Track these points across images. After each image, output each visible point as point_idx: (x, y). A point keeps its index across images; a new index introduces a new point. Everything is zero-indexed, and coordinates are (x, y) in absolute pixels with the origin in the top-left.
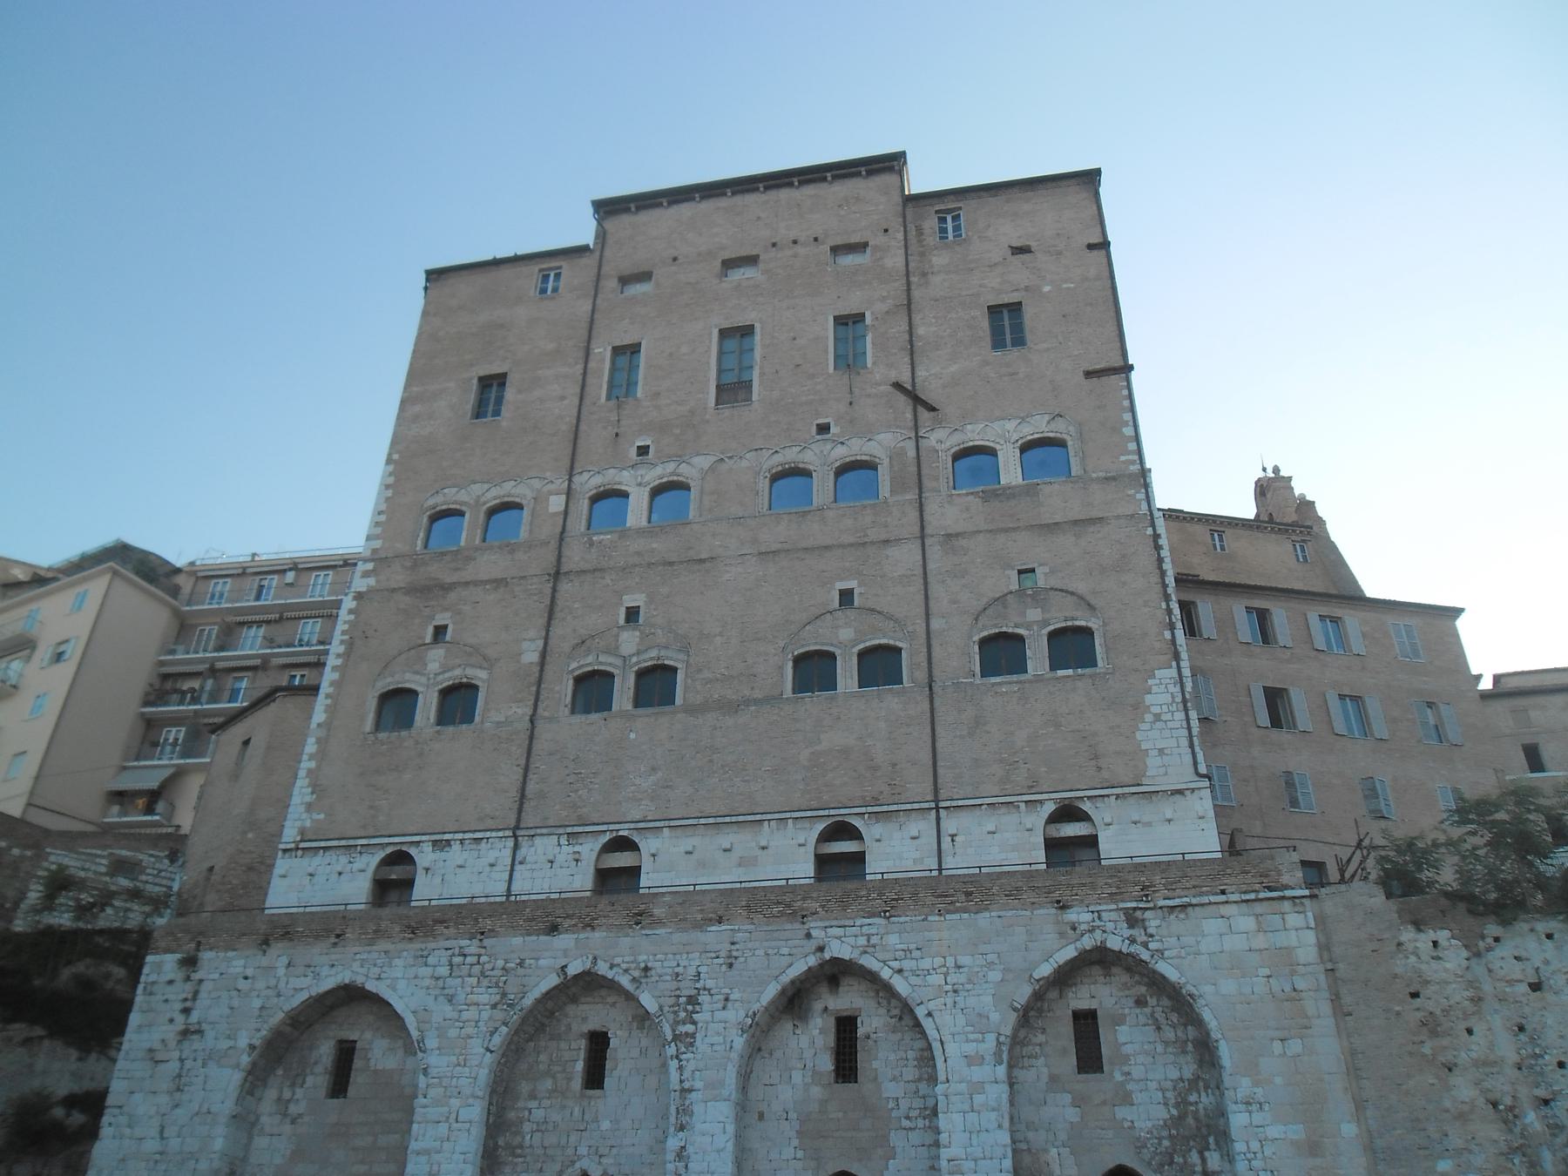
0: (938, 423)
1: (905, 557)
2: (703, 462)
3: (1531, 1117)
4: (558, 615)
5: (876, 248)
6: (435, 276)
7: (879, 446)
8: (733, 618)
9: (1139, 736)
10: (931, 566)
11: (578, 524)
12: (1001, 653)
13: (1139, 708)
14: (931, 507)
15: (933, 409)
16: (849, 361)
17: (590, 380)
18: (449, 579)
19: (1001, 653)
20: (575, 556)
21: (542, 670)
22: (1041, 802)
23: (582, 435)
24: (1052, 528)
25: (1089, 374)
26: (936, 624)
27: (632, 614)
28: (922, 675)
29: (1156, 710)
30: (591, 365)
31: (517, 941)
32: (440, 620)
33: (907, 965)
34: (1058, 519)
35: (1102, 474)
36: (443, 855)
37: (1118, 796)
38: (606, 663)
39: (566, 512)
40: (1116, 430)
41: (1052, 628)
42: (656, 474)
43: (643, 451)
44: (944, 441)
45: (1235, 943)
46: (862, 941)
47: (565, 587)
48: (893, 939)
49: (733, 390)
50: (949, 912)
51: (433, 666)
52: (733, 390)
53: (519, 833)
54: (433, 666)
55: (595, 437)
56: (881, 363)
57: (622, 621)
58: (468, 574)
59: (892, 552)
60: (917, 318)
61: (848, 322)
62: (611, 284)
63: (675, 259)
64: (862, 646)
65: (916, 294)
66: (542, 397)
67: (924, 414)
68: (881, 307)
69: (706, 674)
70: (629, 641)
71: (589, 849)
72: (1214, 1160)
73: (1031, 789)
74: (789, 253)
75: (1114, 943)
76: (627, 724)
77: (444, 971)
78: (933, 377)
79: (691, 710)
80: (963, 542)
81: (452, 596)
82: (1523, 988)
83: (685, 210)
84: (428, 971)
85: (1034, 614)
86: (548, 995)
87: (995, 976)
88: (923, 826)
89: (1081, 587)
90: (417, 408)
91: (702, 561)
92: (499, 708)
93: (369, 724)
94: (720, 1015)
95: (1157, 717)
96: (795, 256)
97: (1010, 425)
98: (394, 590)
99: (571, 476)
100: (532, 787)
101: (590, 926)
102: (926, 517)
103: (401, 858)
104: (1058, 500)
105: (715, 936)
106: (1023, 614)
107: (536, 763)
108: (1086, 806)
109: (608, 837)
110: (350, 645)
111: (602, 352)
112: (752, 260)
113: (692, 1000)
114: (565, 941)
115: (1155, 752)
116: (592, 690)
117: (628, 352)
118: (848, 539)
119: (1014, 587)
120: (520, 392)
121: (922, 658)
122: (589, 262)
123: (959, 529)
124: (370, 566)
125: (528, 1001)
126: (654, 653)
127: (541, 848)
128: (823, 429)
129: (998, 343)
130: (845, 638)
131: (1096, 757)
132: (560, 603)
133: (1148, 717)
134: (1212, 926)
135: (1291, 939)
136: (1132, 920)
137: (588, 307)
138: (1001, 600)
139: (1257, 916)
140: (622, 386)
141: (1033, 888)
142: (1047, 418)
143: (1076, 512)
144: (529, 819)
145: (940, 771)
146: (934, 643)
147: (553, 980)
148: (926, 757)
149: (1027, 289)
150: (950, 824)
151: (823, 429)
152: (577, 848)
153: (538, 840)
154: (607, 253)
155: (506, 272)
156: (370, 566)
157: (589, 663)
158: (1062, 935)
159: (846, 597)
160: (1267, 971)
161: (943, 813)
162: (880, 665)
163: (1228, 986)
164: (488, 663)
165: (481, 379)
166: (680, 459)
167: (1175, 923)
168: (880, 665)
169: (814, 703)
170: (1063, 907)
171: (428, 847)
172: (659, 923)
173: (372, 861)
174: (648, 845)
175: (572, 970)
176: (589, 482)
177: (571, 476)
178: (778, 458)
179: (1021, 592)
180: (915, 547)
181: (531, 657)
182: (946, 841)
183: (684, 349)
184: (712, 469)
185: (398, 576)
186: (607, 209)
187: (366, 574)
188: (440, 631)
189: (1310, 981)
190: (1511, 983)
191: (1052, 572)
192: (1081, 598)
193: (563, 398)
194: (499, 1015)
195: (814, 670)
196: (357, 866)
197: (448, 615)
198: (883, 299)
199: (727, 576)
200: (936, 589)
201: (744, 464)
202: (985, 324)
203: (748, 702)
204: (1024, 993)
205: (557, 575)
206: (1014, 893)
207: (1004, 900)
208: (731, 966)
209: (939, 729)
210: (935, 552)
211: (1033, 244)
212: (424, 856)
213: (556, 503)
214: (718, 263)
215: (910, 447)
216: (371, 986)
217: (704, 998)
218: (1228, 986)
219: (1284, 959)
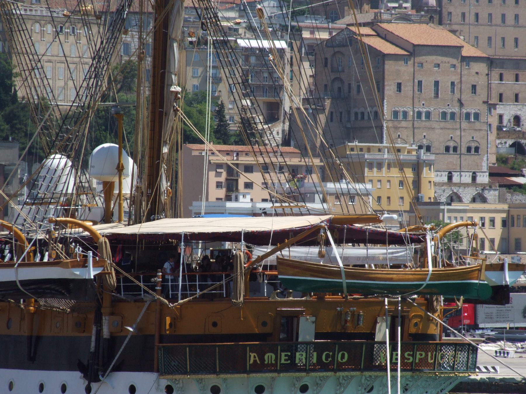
1: (458, 132)
7: (456, 110)
16: (453, 91)
18: (399, 126)
19: (469, 149)
24: (476, 130)
27: (425, 136)
32: (399, 133)
43: (423, 104)
44: (464, 111)
47: (415, 130)
55: (416, 100)
59: (457, 131)
61: (453, 84)
70: (425, 140)
81: (400, 129)
85: (473, 144)
88: (459, 173)
89: (479, 141)
104: (478, 125)
111: (416, 81)
117: (420, 83)
118: (451, 127)
123: (465, 128)
130: (452, 144)
136: (483, 190)
137: (413, 70)
140: (420, 90)
143: (479, 128)
150: (462, 173)
151: (448, 105)
189: (497, 198)
203: (440, 154)
206: (472, 185)
213: (411, 113)
219: (495, 196)
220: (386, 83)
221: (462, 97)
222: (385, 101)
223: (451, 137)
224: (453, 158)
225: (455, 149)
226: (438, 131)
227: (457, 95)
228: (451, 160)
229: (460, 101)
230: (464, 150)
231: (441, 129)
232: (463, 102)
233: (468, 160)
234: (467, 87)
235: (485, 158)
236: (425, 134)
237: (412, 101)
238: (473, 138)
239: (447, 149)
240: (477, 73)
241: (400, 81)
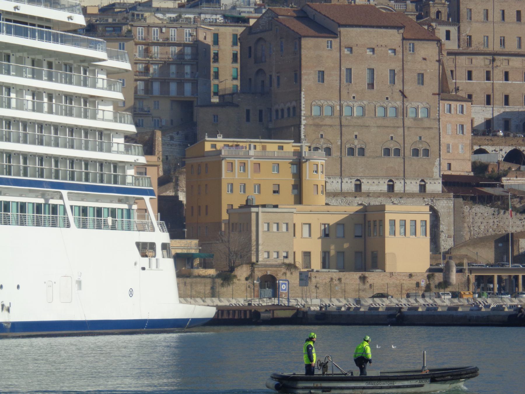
0: (407, 101)
1: (401, 131)
3: (472, 228)
4: (343, 135)
8: (374, 139)
10: (405, 134)
12: (416, 152)
13: (434, 164)
14: (406, 120)
16: (393, 82)
17: (342, 77)
18: (321, 123)
19: (416, 152)
24: (424, 128)
25: (433, 94)
26: (406, 145)
27: (356, 136)
30: (342, 72)
32: (322, 133)
34: (425, 126)
38: (352, 146)
43: (354, 97)
45: (444, 205)
47: (343, 129)
49: (371, 86)
52: (371, 86)
55: (344, 92)
56: (398, 86)
60: (405, 73)
61: (393, 72)
68: (399, 69)
70: (356, 142)
71: (353, 181)
72: (436, 230)
73: (418, 176)
74: (380, 49)
76: (357, 159)
78: (408, 89)
81: (323, 128)
85: (421, 146)
89: (428, 141)
91: (367, 126)
98: (311, 125)
100: (343, 169)
108: (425, 180)
114: (358, 199)
116: (351, 151)
117: (349, 70)
118: (392, 125)
124: (304, 118)
127: (345, 180)
128: (387, 98)
129: (419, 83)
130: (392, 146)
134: (442, 202)
135: (450, 205)
136: (432, 201)
137: (339, 55)
138: (415, 142)
140: (349, 80)
143: (428, 126)
144: (343, 175)
148: (403, 169)
149: (425, 70)
151: (387, 98)
156: (304, 118)
159: (392, 138)
162: (397, 152)
163: (442, 210)
164: (331, 143)
167: (438, 202)
168: (397, 152)
169: (387, 158)
170: (424, 198)
180: (402, 128)
181: (339, 143)
185: (311, 122)
189: (452, 211)
193: (337, 80)
195: (387, 152)
198: (399, 67)
200: (406, 139)
202: (417, 78)
203: (377, 157)
206: (418, 196)
218: (442, 210)
219: (449, 207)
220: (303, 72)
221: (405, 88)
222: (303, 93)
224: (394, 162)
227: (398, 86)
229: (402, 93)
230: (408, 152)
231: (378, 127)
232: (406, 94)
233: (415, 164)
234: (411, 77)
235: (437, 163)
236: (356, 133)
237: (338, 93)
238: (420, 138)
239: (387, 152)
240: (425, 59)
241: (322, 69)
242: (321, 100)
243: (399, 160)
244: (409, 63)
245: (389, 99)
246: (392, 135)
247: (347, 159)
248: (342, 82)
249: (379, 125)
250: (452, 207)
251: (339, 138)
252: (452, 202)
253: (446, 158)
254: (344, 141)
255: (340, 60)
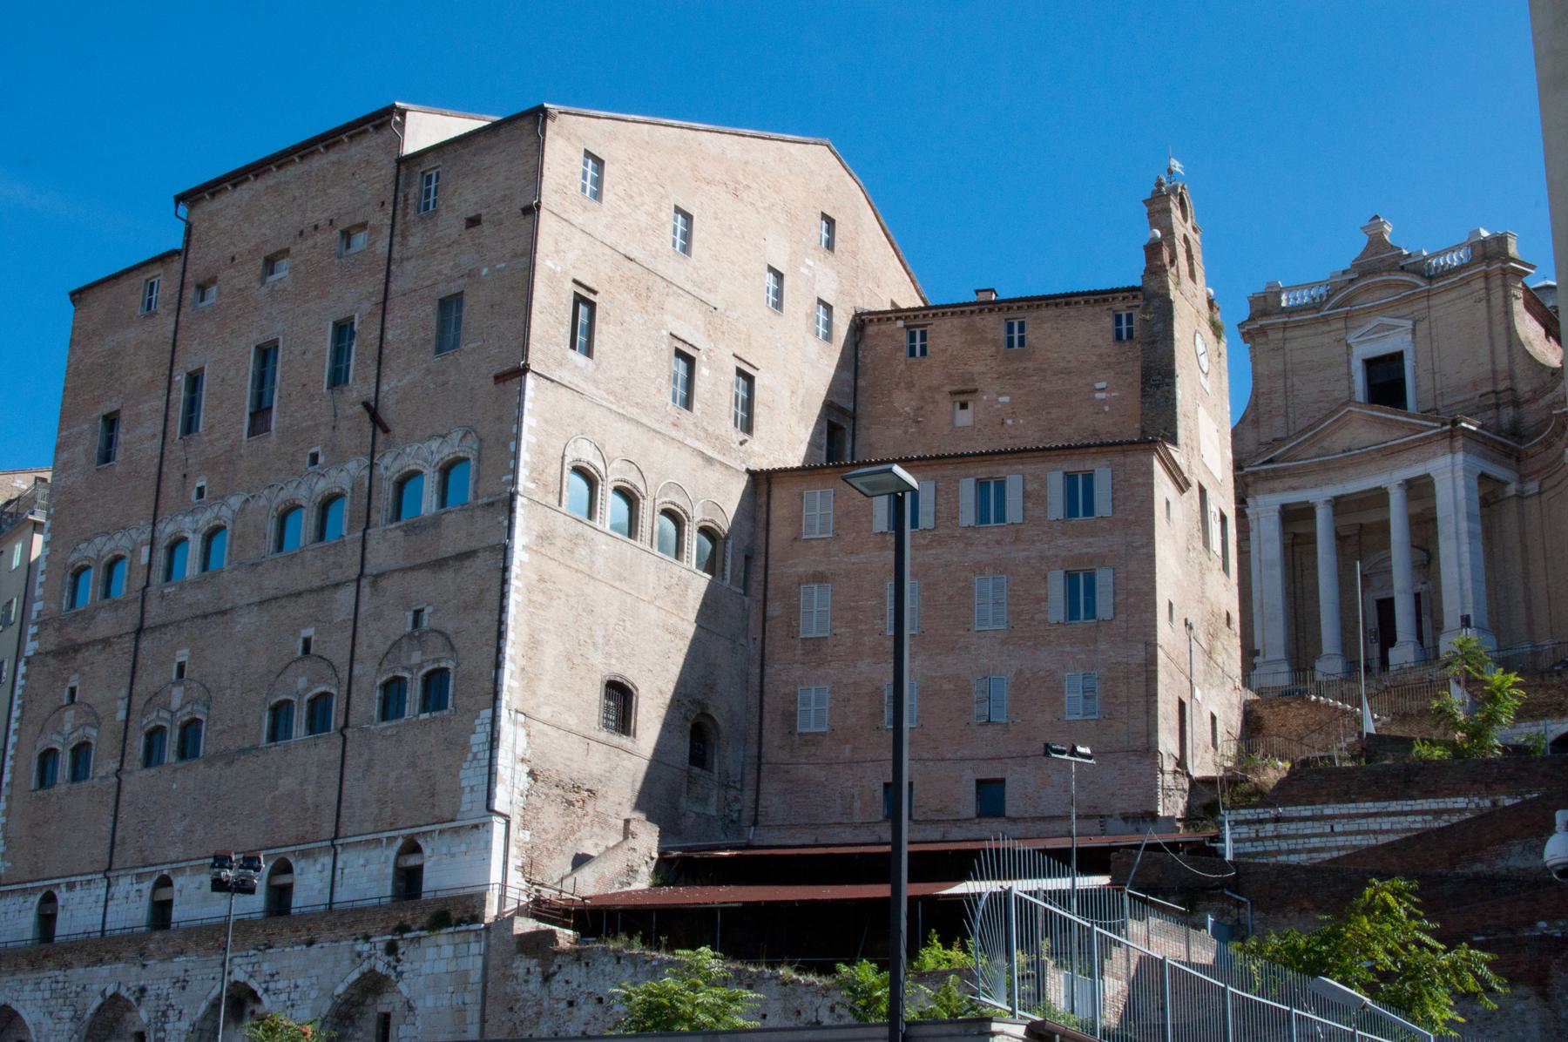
0: (389, 445)
2: (235, 502)
4: (139, 673)
5: (373, 227)
6: (77, 296)
9: (462, 774)
10: (362, 609)
11: (158, 575)
13: (466, 747)
15: (386, 431)
16: (338, 377)
18: (81, 639)
20: (155, 612)
21: (126, 727)
22: (395, 838)
23: (164, 476)
24: (439, 564)
28: (341, 722)
29: (475, 749)
30: (173, 396)
31: (81, 971)
32: (74, 681)
33: (272, 986)
35: (485, 500)
36: (72, 894)
37: (441, 832)
39: (150, 565)
40: (506, 445)
41: (424, 671)
42: (206, 519)
45: (441, 967)
46: (250, 969)
47: (145, 644)
48: (265, 966)
50: (298, 944)
51: (68, 727)
53: (111, 874)
54: (68, 727)
57: (174, 676)
58: (89, 635)
60: (389, 317)
61: (343, 331)
62: (190, 293)
63: (233, 259)
64: (309, 695)
65: (393, 287)
66: (140, 438)
67: (381, 437)
68: (367, 306)
69: (219, 727)
70: (177, 696)
71: (147, 886)
75: (380, 967)
77: (47, 994)
79: (210, 761)
80: (384, 583)
81: (80, 656)
82: (563, 1005)
83: (245, 192)
84: (39, 995)
85: (416, 657)
86: (99, 1009)
87: (313, 994)
89: (449, 627)
90: (65, 456)
92: (103, 765)
93: (33, 783)
94: (178, 1025)
95: (475, 755)
96: (314, 247)
97: (435, 445)
99: (154, 525)
100: (119, 834)
101: (118, 959)
102: (368, 556)
103: (49, 898)
105: (178, 966)
106: (409, 658)
107: (123, 814)
108: (421, 842)
109: (155, 878)
110: (22, 707)
111: (180, 379)
112: (285, 253)
113: (164, 1014)
114: (104, 970)
115: (467, 790)
117: (194, 380)
118: (317, 583)
119: (409, 628)
120: (128, 431)
121: (343, 706)
122: (177, 266)
125: (87, 1016)
126: (189, 708)
127: (124, 885)
131: (433, 795)
132: (140, 660)
133: (470, 756)
134: (431, 953)
139: (456, 944)
141: (343, 924)
142: (460, 434)
143: (462, 547)
144: (117, 863)
145: (343, 811)
146: (354, 688)
147: (99, 1001)
151: (314, 459)
152: (140, 886)
153: (122, 881)
154: (191, 255)
155: (125, 285)
157: (152, 719)
158: (353, 961)
160: (450, 989)
161: (339, 849)
163: (430, 1001)
165: (105, 418)
166: (221, 498)
171: (63, 888)
172: (151, 956)
173: (35, 899)
174: (178, 882)
175: (108, 993)
176: (167, 530)
177: (154, 525)
178: (284, 495)
179: (410, 636)
180: (352, 588)
181: (121, 715)
182: (338, 873)
183: (232, 374)
184: (242, 510)
185: (52, 640)
186: (189, 198)
187: (35, 637)
188: (73, 691)
190: (558, 1000)
191: (435, 611)
192: (448, 638)
194: (73, 1026)
196: (28, 905)
197: (76, 676)
199: (239, 627)
201: (263, 502)
202: (433, 322)
203: (243, 751)
204: (326, 1006)
205: (139, 631)
207: (326, 934)
208: (184, 988)
209: (346, 773)
210: (366, 590)
211: (483, 212)
212: (62, 896)
214: (261, 262)
215: (366, 472)
216: (14, 1006)
217: (170, 1013)
219: (461, 978)
221: (384, 388)
223: (307, 642)
225: (319, 710)
226: (245, 622)
228: (287, 784)
229: (373, 411)
230: (367, 703)
232: (388, 413)
234: (412, 322)
236: (183, 655)
239: (280, 714)
240: (473, 222)
242: (97, 535)
243: (327, 748)
244: (409, 266)
245: (321, 460)
246: (309, 632)
247: (138, 780)
248: (168, 440)
249: (272, 592)
250: (475, 976)
251: (124, 692)
252: (475, 948)
253: (966, 752)
254: (139, 702)
255: (174, 345)
